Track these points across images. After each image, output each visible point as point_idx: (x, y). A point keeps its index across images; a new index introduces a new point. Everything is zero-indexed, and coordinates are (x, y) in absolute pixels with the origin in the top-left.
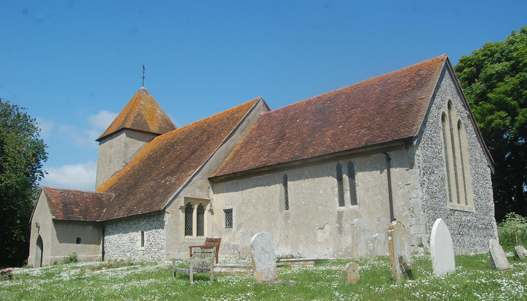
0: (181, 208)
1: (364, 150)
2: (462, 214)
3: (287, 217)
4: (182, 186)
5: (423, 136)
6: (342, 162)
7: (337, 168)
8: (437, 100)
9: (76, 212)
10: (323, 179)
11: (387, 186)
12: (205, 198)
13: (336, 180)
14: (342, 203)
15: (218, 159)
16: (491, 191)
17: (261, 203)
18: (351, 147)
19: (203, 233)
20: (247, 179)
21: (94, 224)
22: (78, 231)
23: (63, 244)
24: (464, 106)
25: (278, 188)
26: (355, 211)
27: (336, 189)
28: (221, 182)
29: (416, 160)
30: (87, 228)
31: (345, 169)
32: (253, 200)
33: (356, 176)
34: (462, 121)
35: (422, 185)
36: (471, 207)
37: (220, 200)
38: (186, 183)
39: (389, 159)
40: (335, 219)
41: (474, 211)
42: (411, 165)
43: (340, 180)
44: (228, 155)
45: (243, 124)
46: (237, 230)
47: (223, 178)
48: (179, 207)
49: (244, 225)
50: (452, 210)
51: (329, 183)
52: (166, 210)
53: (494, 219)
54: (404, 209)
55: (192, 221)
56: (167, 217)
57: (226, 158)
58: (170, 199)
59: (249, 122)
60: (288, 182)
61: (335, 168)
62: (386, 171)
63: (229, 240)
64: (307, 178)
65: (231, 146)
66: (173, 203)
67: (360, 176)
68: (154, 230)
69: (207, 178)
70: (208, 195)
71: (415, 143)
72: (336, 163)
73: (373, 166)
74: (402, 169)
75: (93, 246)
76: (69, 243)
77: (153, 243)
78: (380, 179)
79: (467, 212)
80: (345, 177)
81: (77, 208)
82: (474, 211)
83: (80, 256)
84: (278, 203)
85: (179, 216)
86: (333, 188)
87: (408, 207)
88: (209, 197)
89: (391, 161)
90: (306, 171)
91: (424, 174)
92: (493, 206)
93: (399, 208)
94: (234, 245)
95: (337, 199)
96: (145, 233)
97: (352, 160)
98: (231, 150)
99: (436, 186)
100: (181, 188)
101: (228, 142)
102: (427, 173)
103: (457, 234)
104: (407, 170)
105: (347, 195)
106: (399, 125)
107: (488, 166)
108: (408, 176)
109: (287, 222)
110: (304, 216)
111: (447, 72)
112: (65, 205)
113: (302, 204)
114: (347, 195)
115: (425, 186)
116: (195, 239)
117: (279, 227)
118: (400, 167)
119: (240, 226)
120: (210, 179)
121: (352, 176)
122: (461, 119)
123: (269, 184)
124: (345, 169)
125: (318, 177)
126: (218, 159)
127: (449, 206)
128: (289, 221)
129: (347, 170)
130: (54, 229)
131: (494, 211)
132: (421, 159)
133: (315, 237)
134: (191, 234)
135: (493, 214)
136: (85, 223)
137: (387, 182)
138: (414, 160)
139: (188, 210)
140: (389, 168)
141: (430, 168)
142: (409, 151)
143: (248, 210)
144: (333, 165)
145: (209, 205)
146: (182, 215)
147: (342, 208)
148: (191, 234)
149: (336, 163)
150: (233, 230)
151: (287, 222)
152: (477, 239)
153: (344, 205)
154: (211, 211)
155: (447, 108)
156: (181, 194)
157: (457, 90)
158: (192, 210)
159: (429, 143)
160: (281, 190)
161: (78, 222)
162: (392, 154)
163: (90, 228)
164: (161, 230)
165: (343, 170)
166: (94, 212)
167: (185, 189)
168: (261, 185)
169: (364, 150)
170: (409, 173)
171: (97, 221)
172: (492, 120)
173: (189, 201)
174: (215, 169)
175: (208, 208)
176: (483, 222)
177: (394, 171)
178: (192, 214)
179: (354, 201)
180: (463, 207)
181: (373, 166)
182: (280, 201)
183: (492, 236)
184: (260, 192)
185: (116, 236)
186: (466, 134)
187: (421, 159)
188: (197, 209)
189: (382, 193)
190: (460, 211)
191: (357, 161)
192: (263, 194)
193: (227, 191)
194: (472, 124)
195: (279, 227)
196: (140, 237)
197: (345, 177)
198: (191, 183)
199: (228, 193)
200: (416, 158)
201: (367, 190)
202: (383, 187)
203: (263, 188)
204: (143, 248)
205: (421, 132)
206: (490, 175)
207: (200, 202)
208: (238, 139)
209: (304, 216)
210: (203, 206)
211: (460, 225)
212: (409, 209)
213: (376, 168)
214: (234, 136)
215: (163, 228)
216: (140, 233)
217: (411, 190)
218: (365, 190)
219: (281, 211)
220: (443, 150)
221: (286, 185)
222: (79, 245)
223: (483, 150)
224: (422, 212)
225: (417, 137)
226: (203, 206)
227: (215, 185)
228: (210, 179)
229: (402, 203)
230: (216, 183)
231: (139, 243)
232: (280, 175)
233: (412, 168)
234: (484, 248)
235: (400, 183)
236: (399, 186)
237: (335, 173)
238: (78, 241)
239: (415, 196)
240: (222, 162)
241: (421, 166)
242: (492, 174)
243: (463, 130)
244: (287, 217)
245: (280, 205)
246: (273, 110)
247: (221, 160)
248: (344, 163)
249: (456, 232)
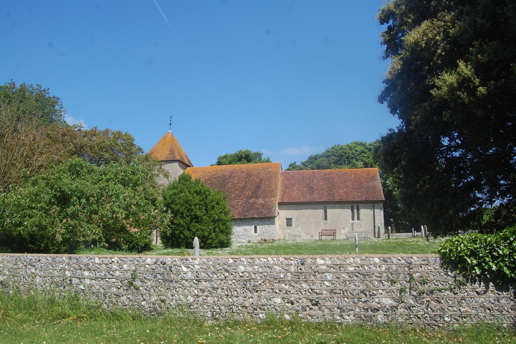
3: (326, 223)
6: (354, 205)
14: (353, 219)
31: (355, 207)
39: (374, 206)
40: (350, 225)
64: (337, 208)
80: (355, 210)
84: (321, 217)
90: (337, 206)
96: (258, 227)
105: (356, 217)
114: (356, 217)
119: (297, 226)
123: (316, 209)
124: (355, 207)
133: (341, 232)
144: (350, 205)
147: (353, 221)
162: (375, 204)
179: (358, 219)
191: (361, 205)
196: (254, 229)
197: (355, 210)
199: (289, 211)
201: (365, 216)
216: (254, 226)
228: (280, 204)
232: (323, 206)
248: (355, 206)
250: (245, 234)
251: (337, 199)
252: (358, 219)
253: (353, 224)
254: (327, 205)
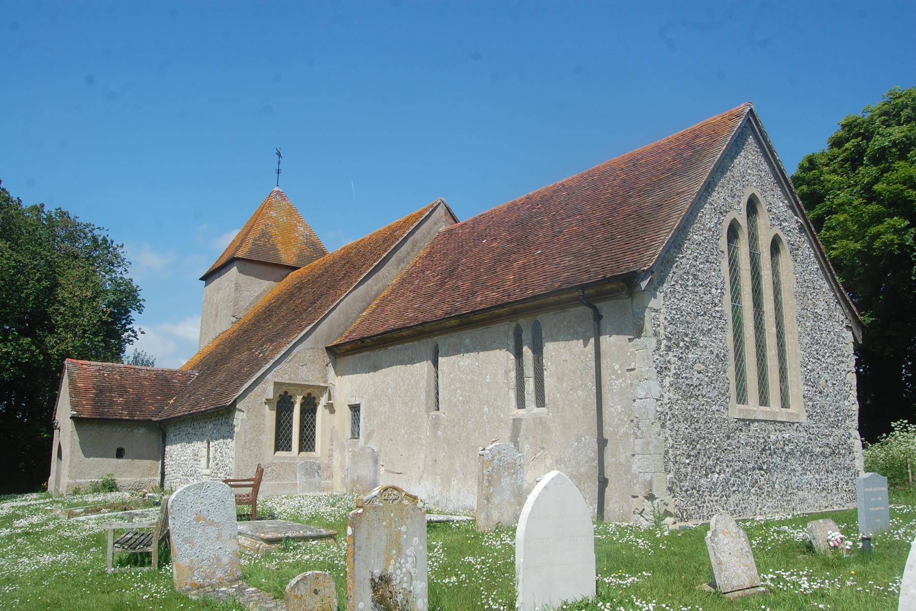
0: (268, 402)
1: (556, 298)
2: (771, 427)
4: (272, 362)
5: (674, 269)
6: (522, 321)
7: (515, 334)
8: (718, 196)
9: (117, 404)
10: (491, 353)
11: (593, 372)
12: (317, 383)
13: (512, 357)
15: (347, 313)
16: (852, 379)
17: (399, 396)
18: (538, 291)
19: (314, 447)
20: (383, 351)
21: (147, 424)
22: (118, 437)
23: (91, 459)
24: (791, 207)
25: (425, 367)
27: (513, 374)
28: (347, 355)
29: (647, 319)
30: (136, 431)
33: (545, 350)
34: (784, 238)
35: (661, 371)
36: (797, 410)
37: (346, 387)
38: (279, 356)
39: (598, 317)
41: (803, 419)
42: (638, 331)
43: (519, 355)
44: (370, 304)
45: (403, 248)
47: (348, 347)
48: (264, 400)
49: (375, 435)
50: (743, 420)
51: (500, 360)
52: (237, 406)
53: (856, 434)
54: (622, 420)
55: (291, 426)
56: (239, 418)
57: (364, 310)
58: (246, 386)
59: (414, 244)
60: (440, 359)
61: (511, 333)
62: (592, 340)
65: (375, 288)
66: (252, 394)
67: (550, 349)
68: (222, 440)
69: (323, 347)
70: (325, 378)
71: (644, 284)
72: (514, 324)
73: (572, 331)
74: (621, 337)
75: (147, 463)
76: (102, 456)
77: (220, 464)
78: (582, 358)
79: (783, 422)
80: (527, 352)
81: (122, 396)
82: (803, 419)
83: (120, 480)
84: (423, 397)
85: (263, 415)
86: (507, 372)
87: (630, 415)
88: (326, 382)
89: (602, 322)
90: (467, 337)
91: (669, 348)
92: (856, 407)
93: (613, 418)
95: (512, 394)
97: (538, 318)
98: (376, 296)
99: (699, 372)
100: (268, 366)
101: (370, 281)
102: (678, 345)
103: (754, 469)
104: (630, 340)
105: (530, 386)
106: (627, 246)
107: (847, 327)
108: (632, 353)
109: (435, 434)
111: (751, 139)
112: (100, 391)
113: (458, 400)
114: (530, 386)
115: (671, 374)
116: (294, 458)
117: (424, 442)
118: (618, 334)
120: (329, 350)
121: (538, 351)
122: (781, 234)
124: (527, 336)
125: (484, 350)
126: (347, 313)
127: (735, 411)
129: (530, 337)
130: (75, 433)
131: (856, 418)
132: (662, 317)
134: (289, 448)
135: (856, 424)
136: (132, 423)
137: (594, 364)
138: (643, 319)
139: (283, 405)
140: (598, 334)
141: (687, 335)
142: (635, 302)
143: (381, 409)
144: (506, 328)
145: (326, 396)
146: (270, 416)
147: (521, 411)
148: (289, 448)
149: (514, 324)
151: (435, 434)
152: (809, 476)
153: (524, 407)
154: (331, 408)
155: (744, 212)
156: (269, 376)
157: (776, 176)
158: (292, 405)
159: (689, 283)
160: (428, 372)
161: (119, 422)
162: (605, 307)
163: (142, 430)
164: (229, 440)
165: (524, 337)
166: (152, 404)
167: (279, 367)
168: (402, 363)
169: (556, 298)
170: (635, 345)
171: (154, 419)
172: (877, 235)
173: (284, 389)
174: (340, 331)
175: (323, 401)
176: (825, 441)
177: (607, 341)
178: (292, 411)
180: (774, 413)
181: (572, 331)
182: (427, 393)
183: (849, 469)
185: (179, 446)
186: (792, 263)
187: (662, 317)
188: (302, 405)
189: (586, 386)
190: (766, 421)
191: (547, 320)
193: (355, 372)
194: (811, 244)
195: (424, 442)
197: (527, 352)
198: (290, 358)
200: (648, 315)
201: (561, 379)
202: (587, 375)
203: (403, 367)
205: (666, 262)
206: (851, 346)
207: (309, 391)
208: (391, 274)
210: (314, 398)
211: (763, 450)
212: (632, 421)
213: (577, 333)
214: (384, 270)
215: (232, 438)
217: (636, 382)
218: (558, 378)
219: (428, 412)
220: (728, 297)
221: (436, 364)
222: (120, 461)
223: (835, 295)
224: (657, 428)
225: (650, 271)
226: (314, 398)
227: (338, 360)
228: (329, 350)
229: (619, 407)
230: (339, 357)
231: (204, 461)
232: (426, 346)
233: (639, 337)
234: (824, 494)
235: (617, 367)
236: (614, 372)
237: (511, 343)
238: (120, 454)
239: (643, 395)
240: (355, 319)
241: (662, 332)
242: (855, 343)
243: (785, 258)
244: (436, 424)
245: (427, 400)
246: (462, 220)
247: (354, 315)
249: (751, 466)
254: (440, 340)
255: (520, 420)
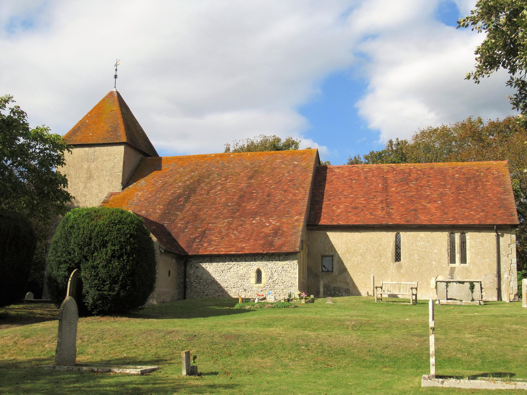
14: (452, 260)
26: (466, 268)
32: (361, 251)
40: (448, 272)
46: (339, 274)
63: (329, 282)
94: (335, 287)
105: (458, 257)
110: (418, 267)
114: (458, 257)
128: (402, 271)
147: (453, 265)
150: (334, 274)
184: (370, 244)
192: (372, 246)
204: (260, 285)
209: (418, 267)
231: (253, 280)
250: (239, 284)
251: (423, 219)
252: (463, 260)
253: (452, 270)
255: (455, 268)
